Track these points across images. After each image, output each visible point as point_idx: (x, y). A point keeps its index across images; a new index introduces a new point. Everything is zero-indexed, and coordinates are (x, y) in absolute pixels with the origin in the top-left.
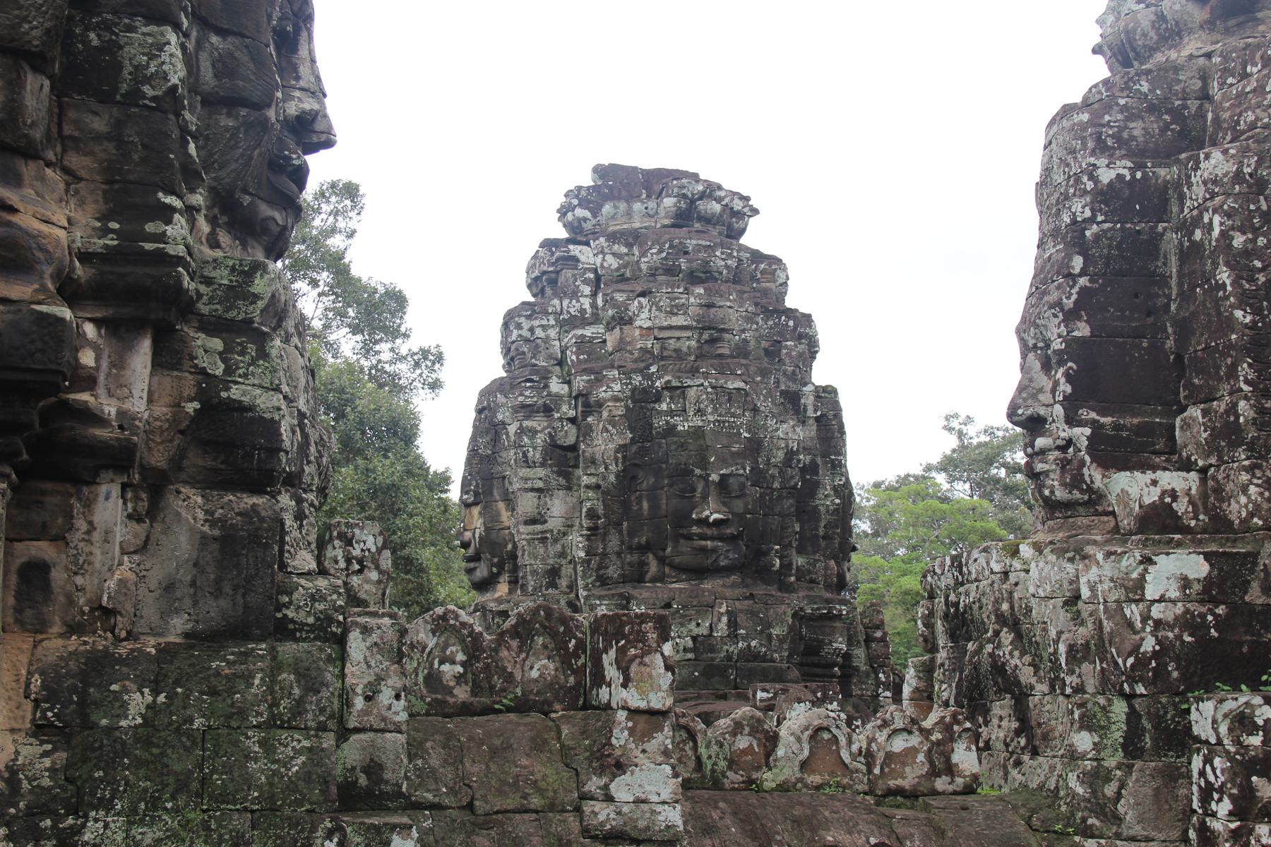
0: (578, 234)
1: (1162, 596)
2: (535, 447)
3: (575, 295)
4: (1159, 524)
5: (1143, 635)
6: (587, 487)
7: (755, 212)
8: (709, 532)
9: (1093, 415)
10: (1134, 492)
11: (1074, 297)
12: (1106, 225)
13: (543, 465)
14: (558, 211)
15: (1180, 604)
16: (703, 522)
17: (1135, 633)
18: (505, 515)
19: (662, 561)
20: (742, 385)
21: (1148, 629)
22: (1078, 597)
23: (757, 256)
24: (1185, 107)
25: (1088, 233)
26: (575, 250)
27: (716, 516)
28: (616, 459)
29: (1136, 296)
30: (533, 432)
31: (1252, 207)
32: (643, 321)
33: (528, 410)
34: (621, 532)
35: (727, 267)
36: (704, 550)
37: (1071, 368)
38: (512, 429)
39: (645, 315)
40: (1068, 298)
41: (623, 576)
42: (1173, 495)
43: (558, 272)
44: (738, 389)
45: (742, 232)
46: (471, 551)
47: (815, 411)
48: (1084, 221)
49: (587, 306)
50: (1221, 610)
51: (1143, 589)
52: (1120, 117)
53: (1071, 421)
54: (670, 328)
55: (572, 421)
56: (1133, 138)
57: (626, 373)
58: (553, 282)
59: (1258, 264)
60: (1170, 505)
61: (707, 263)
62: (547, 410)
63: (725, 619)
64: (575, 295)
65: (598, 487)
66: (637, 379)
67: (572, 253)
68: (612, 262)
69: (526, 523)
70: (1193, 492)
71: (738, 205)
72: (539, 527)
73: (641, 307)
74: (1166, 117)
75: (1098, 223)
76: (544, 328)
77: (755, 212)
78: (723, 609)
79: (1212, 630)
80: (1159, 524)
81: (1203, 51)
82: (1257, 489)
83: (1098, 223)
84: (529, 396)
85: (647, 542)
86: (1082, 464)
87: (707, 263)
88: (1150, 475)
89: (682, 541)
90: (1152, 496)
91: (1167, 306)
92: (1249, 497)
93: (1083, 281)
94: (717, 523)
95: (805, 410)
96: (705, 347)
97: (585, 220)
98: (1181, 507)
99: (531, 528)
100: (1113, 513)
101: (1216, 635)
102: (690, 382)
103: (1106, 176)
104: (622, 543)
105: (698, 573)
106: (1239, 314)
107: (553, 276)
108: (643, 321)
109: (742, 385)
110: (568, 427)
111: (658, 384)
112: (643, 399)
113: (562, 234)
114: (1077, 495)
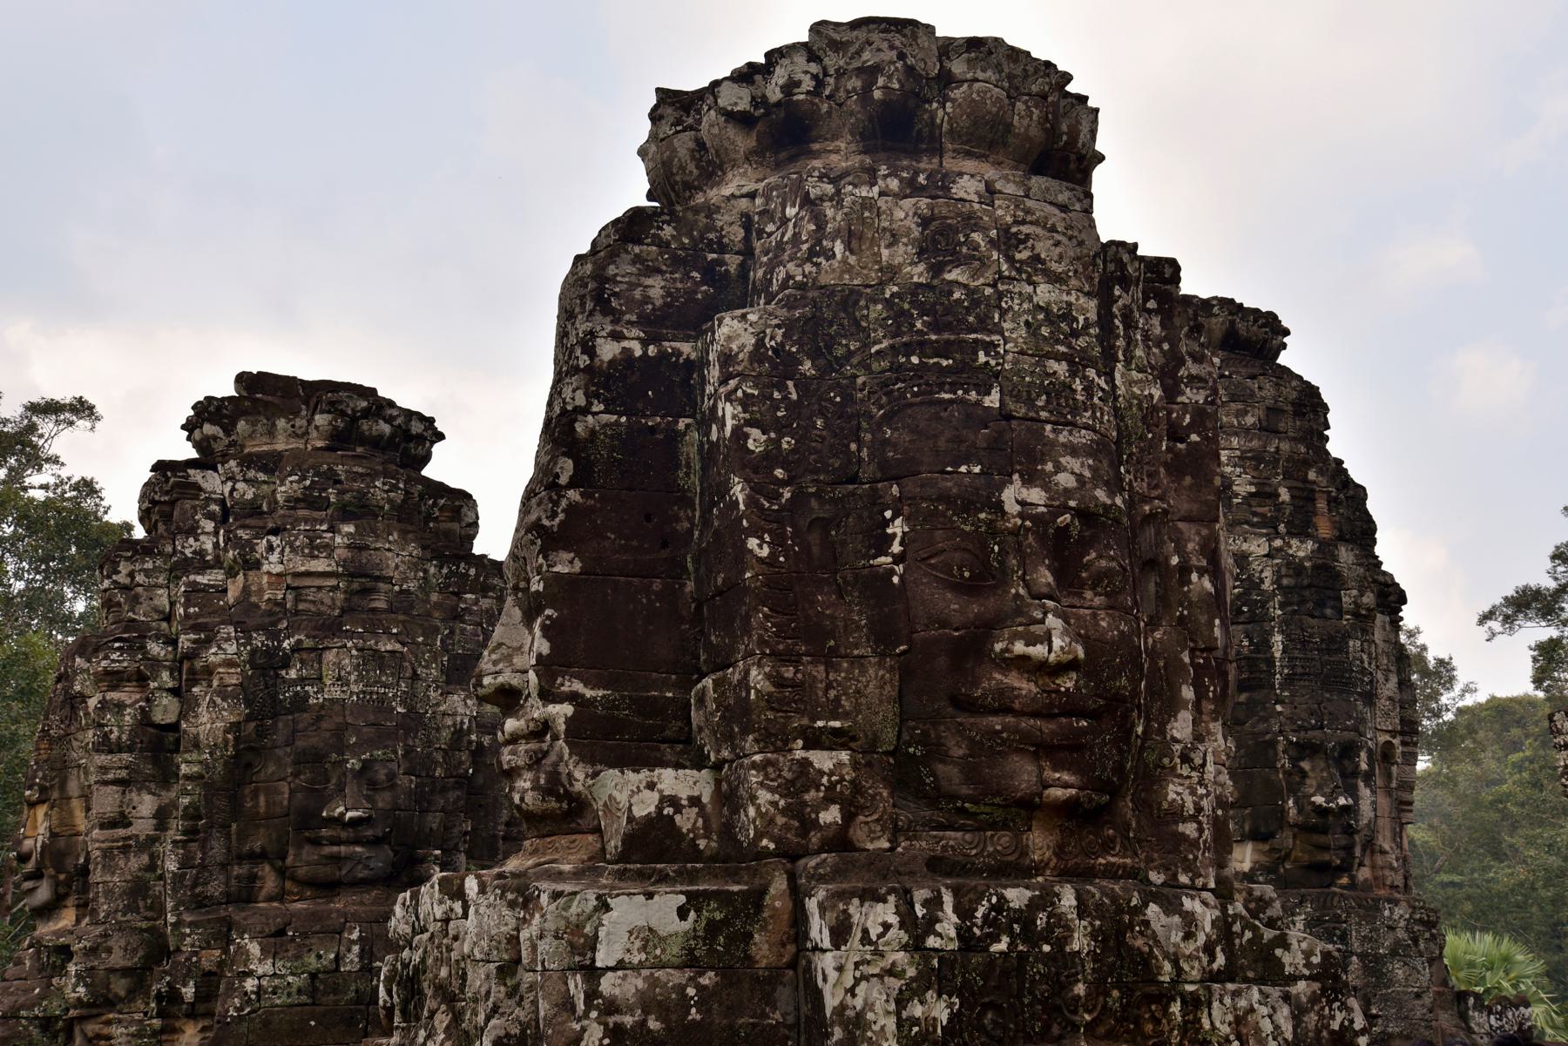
0: (208, 459)
1: (621, 961)
2: (120, 727)
3: (193, 531)
4: (652, 850)
5: (585, 1022)
6: (188, 778)
7: (441, 437)
8: (344, 835)
9: (578, 686)
10: (622, 798)
11: (561, 516)
12: (606, 418)
13: (130, 750)
14: (183, 427)
15: (645, 972)
16: (338, 821)
17: (579, 1020)
18: (79, 815)
19: (282, 873)
20: (398, 647)
21: (594, 1014)
22: (518, 961)
23: (440, 489)
24: (721, 263)
25: (579, 427)
26: (196, 475)
27: (349, 814)
29: (648, 518)
30: (120, 706)
31: (776, 395)
32: (273, 565)
33: (114, 679)
34: (228, 836)
35: (390, 501)
36: (336, 859)
37: (549, 617)
38: (93, 703)
39: (274, 557)
40: (554, 515)
41: (227, 894)
42: (673, 801)
43: (172, 503)
45: (426, 458)
46: (30, 866)
48: (575, 408)
49: (209, 546)
50: (707, 979)
51: (594, 949)
52: (630, 269)
53: (547, 696)
54: (308, 574)
55: (175, 692)
56: (647, 299)
57: (245, 630)
58: (167, 518)
59: (779, 473)
60: (671, 819)
61: (365, 494)
62: (141, 679)
63: (356, 949)
64: (193, 531)
65: (201, 777)
66: (259, 640)
67: (192, 479)
68: (247, 492)
69: (102, 826)
70: (705, 799)
71: (416, 428)
72: (121, 832)
73: (270, 548)
74: (695, 274)
75: (595, 414)
76: (147, 573)
77: (441, 437)
78: (355, 936)
79: (693, 1010)
80: (652, 850)
81: (745, 190)
82: (769, 796)
83: (595, 414)
84: (117, 659)
85: (263, 848)
86: (561, 758)
87: (365, 494)
88: (644, 774)
89: (307, 848)
90: (645, 806)
91: (690, 532)
92: (758, 807)
93: (574, 495)
94: (354, 822)
96: (355, 599)
97: (215, 438)
98: (686, 821)
99: (108, 833)
100: (598, 830)
101: (698, 1017)
103: (608, 350)
104: (229, 850)
105: (328, 888)
106: (753, 543)
107: (166, 508)
108: (273, 565)
109: (398, 647)
110: (166, 700)
111: (285, 645)
112: (267, 665)
113: (189, 452)
114: (553, 804)
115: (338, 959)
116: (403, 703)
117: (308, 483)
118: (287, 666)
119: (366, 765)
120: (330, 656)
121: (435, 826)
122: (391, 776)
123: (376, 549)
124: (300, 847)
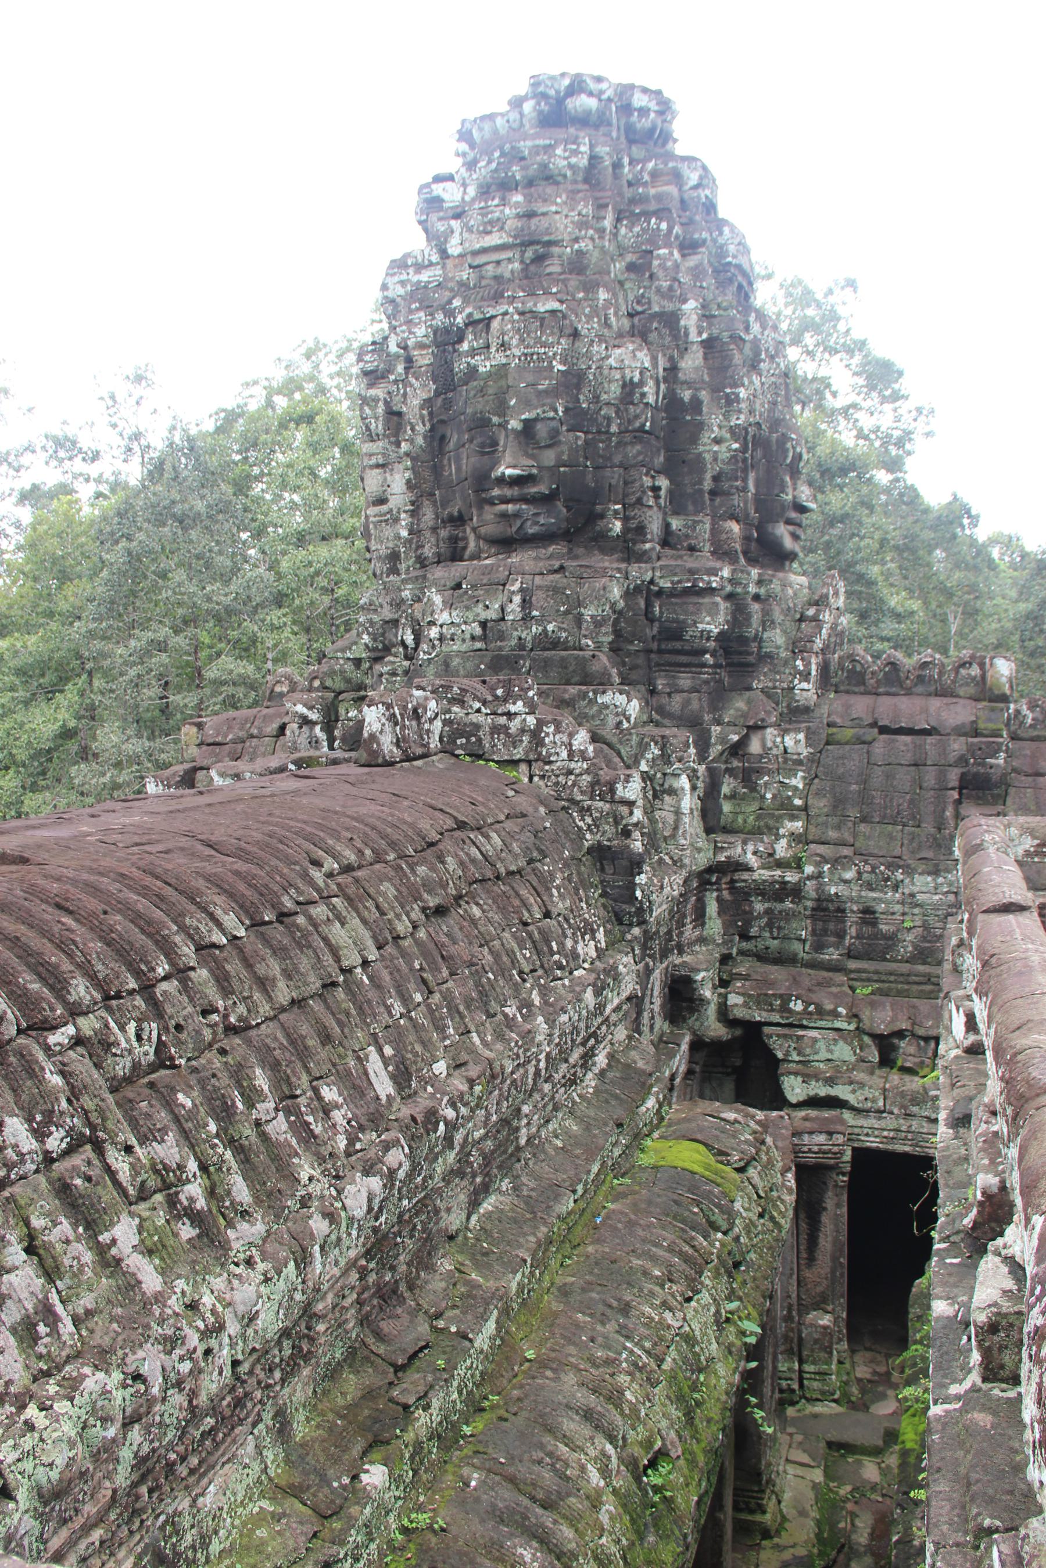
8: (508, 492)
28: (422, 417)
35: (571, 166)
44: (553, 312)
47: (700, 334)
54: (484, 251)
78: (516, 587)
89: (487, 508)
95: (687, 334)
102: (491, 312)
109: (555, 305)
115: (502, 609)
116: (563, 362)
117: (494, 165)
118: (460, 340)
119: (528, 425)
120: (495, 324)
121: (613, 482)
122: (554, 434)
123: (544, 214)
124: (480, 508)
